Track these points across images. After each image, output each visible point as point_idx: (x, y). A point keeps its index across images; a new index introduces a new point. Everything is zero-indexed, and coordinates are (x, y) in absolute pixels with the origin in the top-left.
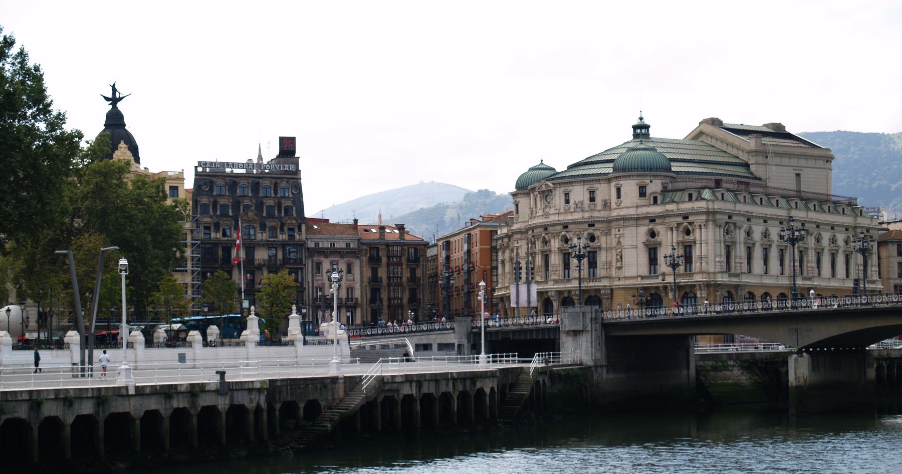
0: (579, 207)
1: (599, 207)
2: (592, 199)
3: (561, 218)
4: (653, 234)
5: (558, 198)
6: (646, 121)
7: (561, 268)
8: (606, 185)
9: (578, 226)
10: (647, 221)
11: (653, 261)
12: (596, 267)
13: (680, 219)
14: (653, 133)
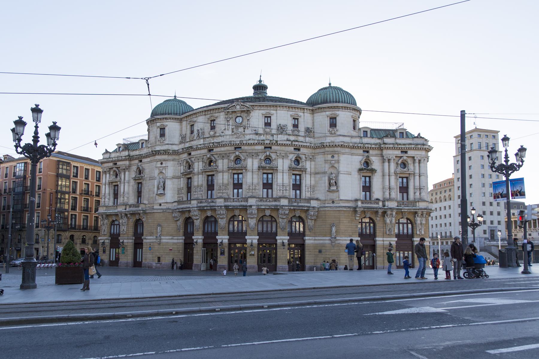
0: (281, 129)
1: (302, 133)
2: (296, 126)
4: (367, 163)
8: (309, 115)
9: (283, 148)
10: (361, 151)
11: (367, 188)
13: (398, 153)
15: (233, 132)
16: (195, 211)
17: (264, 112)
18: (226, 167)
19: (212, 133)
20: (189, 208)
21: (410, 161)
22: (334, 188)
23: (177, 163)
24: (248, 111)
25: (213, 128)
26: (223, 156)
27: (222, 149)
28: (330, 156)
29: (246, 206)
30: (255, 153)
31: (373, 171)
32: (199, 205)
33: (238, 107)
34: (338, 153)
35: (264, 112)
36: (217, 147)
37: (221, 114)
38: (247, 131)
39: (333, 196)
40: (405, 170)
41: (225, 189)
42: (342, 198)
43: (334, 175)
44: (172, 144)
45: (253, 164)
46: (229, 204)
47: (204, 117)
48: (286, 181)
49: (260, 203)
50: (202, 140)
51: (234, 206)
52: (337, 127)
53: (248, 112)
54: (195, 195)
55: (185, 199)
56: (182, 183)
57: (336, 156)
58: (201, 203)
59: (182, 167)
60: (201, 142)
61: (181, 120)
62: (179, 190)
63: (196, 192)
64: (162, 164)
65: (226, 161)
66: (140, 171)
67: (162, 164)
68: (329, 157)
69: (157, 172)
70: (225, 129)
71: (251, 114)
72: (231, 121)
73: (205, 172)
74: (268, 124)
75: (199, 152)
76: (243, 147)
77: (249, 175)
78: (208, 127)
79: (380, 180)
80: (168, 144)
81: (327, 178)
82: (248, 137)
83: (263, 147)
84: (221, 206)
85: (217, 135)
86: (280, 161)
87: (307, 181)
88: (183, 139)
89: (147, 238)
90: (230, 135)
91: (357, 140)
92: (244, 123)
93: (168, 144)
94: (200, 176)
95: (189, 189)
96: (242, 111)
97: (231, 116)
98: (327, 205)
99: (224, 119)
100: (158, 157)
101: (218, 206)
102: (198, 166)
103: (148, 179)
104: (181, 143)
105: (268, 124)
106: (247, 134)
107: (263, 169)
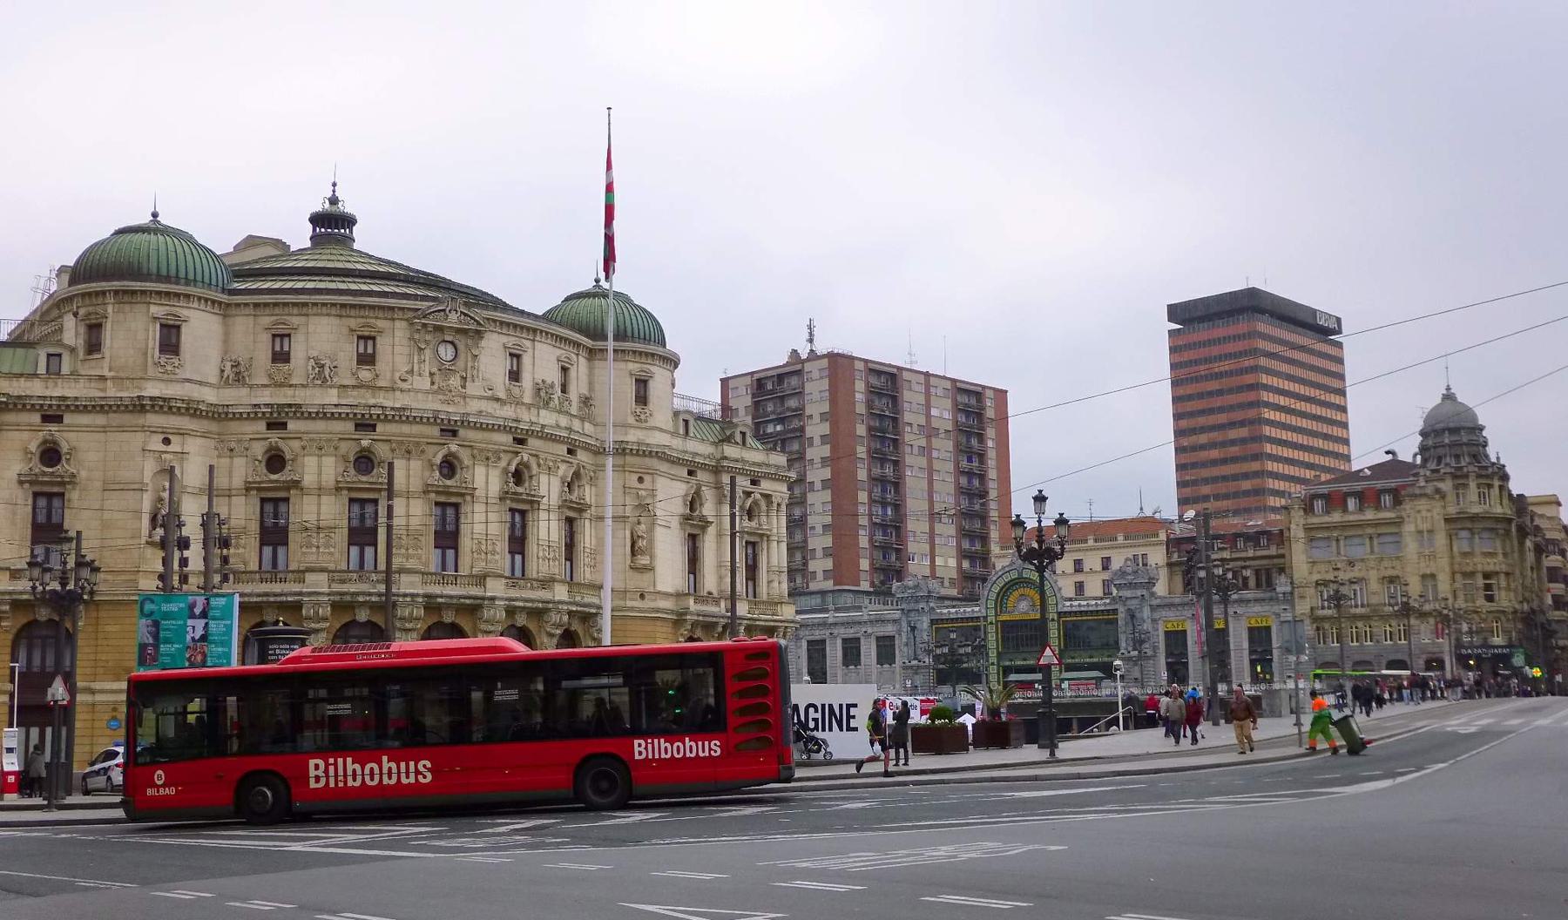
3: (353, 398)
5: (492, 355)
6: (348, 207)
7: (503, 546)
12: (285, 543)
14: (364, 238)
15: (433, 383)
16: (319, 604)
17: (510, 341)
18: (416, 485)
19: (365, 375)
20: (300, 594)
21: (764, 507)
22: (643, 560)
23: (212, 443)
24: (478, 332)
25: (367, 359)
27: (406, 429)
28: (635, 477)
29: (483, 598)
30: (496, 452)
31: (705, 524)
32: (337, 588)
33: (453, 317)
34: (653, 473)
35: (510, 341)
36: (393, 420)
37: (398, 324)
38: (472, 389)
39: (642, 581)
40: (754, 524)
41: (416, 547)
42: (660, 588)
43: (643, 527)
44: (201, 383)
45: (486, 480)
46: (436, 589)
47: (335, 321)
48: (555, 536)
49: (513, 593)
50: (335, 391)
51: (451, 597)
52: (651, 406)
53: (479, 334)
54: (297, 553)
55: (254, 566)
57: (647, 478)
58: (343, 582)
59: (240, 462)
60: (331, 397)
61: (225, 310)
63: (309, 546)
64: (167, 441)
65: (416, 465)
66: (51, 454)
67: (167, 441)
68: (632, 480)
69: (150, 467)
70: (411, 372)
71: (483, 343)
72: (427, 352)
73: (350, 489)
74: (515, 376)
75: (320, 425)
76: (462, 432)
77: (479, 508)
78: (347, 353)
79: (714, 546)
80: (189, 381)
81: (628, 533)
82: (474, 406)
83: (510, 438)
84: (413, 595)
85: (381, 383)
86: (544, 479)
87: (587, 535)
88: (237, 375)
89: (97, 686)
90: (427, 392)
91: (677, 443)
92: (460, 363)
93: (189, 381)
94: (324, 499)
96: (459, 331)
97: (428, 337)
98: (629, 604)
99: (405, 342)
100: (153, 419)
101: (405, 595)
102: (318, 469)
103: (98, 484)
104: (224, 382)
105: (515, 376)
106: (473, 397)
107: (513, 500)
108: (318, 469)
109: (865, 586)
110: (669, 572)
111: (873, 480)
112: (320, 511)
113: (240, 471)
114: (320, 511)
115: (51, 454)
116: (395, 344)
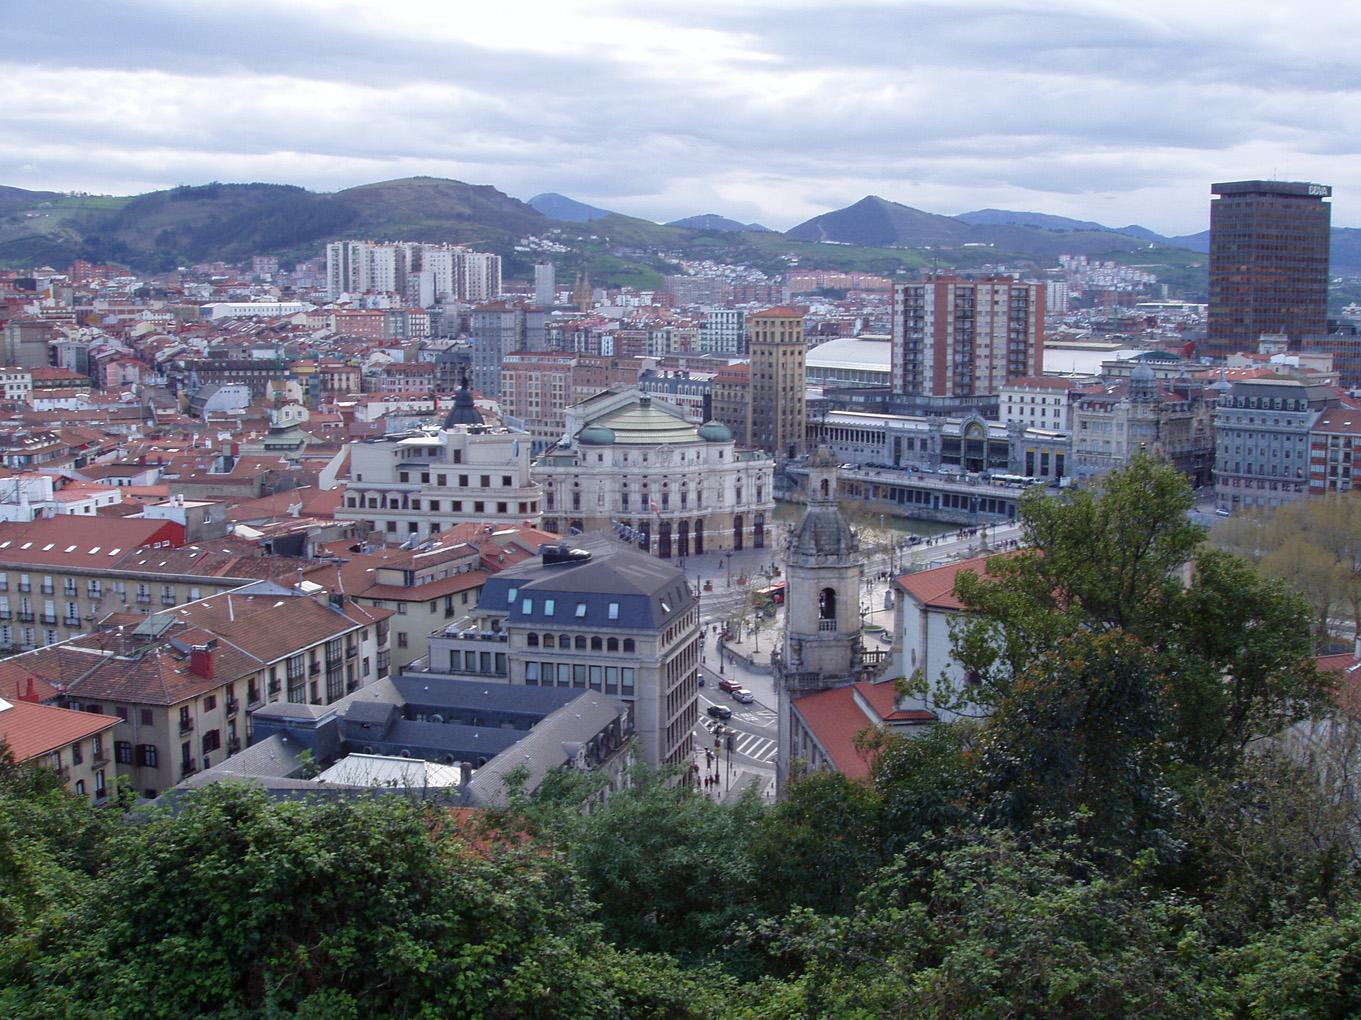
5: (677, 456)
26: (655, 482)
56: (619, 497)
62: (615, 502)
78: (641, 458)
87: (705, 495)
88: (615, 464)
95: (625, 501)
102: (635, 487)
108: (635, 487)
109: (949, 394)
110: (730, 498)
111: (956, 341)
112: (635, 498)
113: (617, 486)
114: (635, 498)
115: (576, 485)
116: (652, 457)
